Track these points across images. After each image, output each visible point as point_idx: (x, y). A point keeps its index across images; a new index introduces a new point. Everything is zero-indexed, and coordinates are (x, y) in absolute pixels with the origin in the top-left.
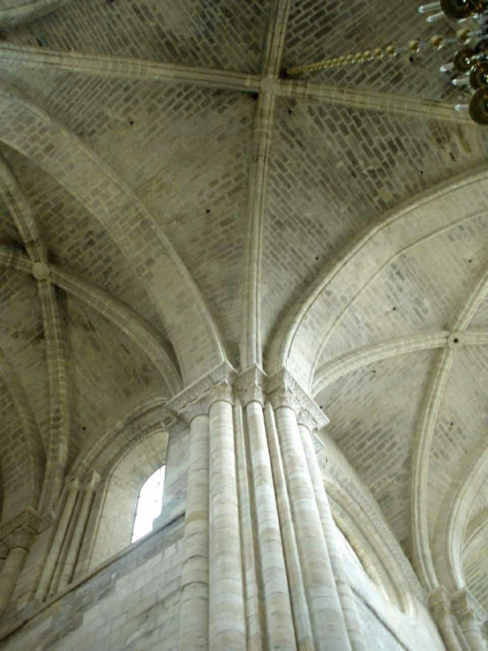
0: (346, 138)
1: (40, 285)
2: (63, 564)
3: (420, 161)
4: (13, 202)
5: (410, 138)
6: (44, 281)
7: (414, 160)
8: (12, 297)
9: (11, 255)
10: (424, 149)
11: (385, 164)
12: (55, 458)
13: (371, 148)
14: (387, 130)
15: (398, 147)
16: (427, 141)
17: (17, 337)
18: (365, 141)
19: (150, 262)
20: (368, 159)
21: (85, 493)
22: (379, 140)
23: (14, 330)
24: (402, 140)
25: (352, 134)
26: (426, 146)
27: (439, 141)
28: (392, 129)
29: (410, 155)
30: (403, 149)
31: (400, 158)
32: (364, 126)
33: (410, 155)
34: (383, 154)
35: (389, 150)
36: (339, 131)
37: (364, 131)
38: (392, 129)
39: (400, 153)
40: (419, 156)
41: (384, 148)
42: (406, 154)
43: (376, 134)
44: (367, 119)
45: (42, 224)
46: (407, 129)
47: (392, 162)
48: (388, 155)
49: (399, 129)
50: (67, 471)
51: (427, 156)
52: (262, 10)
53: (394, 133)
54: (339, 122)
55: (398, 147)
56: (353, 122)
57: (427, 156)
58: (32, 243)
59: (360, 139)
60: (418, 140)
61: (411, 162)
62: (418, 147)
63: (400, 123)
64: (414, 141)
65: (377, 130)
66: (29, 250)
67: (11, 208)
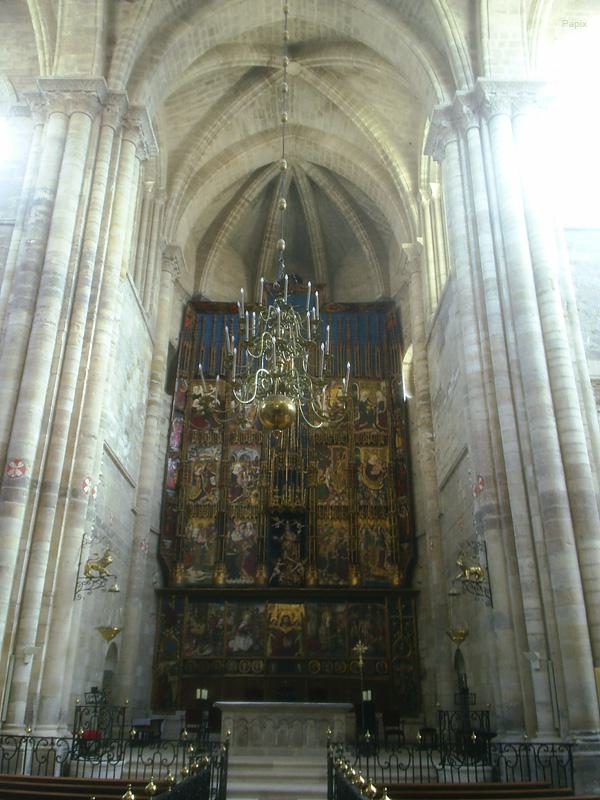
1: (302, 76)
2: (440, 276)
4: (231, 63)
6: (301, 72)
8: (295, 94)
9: (267, 80)
12: (402, 189)
17: (321, 114)
19: (348, 20)
21: (434, 204)
23: (316, 113)
45: (258, 47)
50: (416, 193)
58: (268, 63)
66: (273, 66)
67: (234, 65)
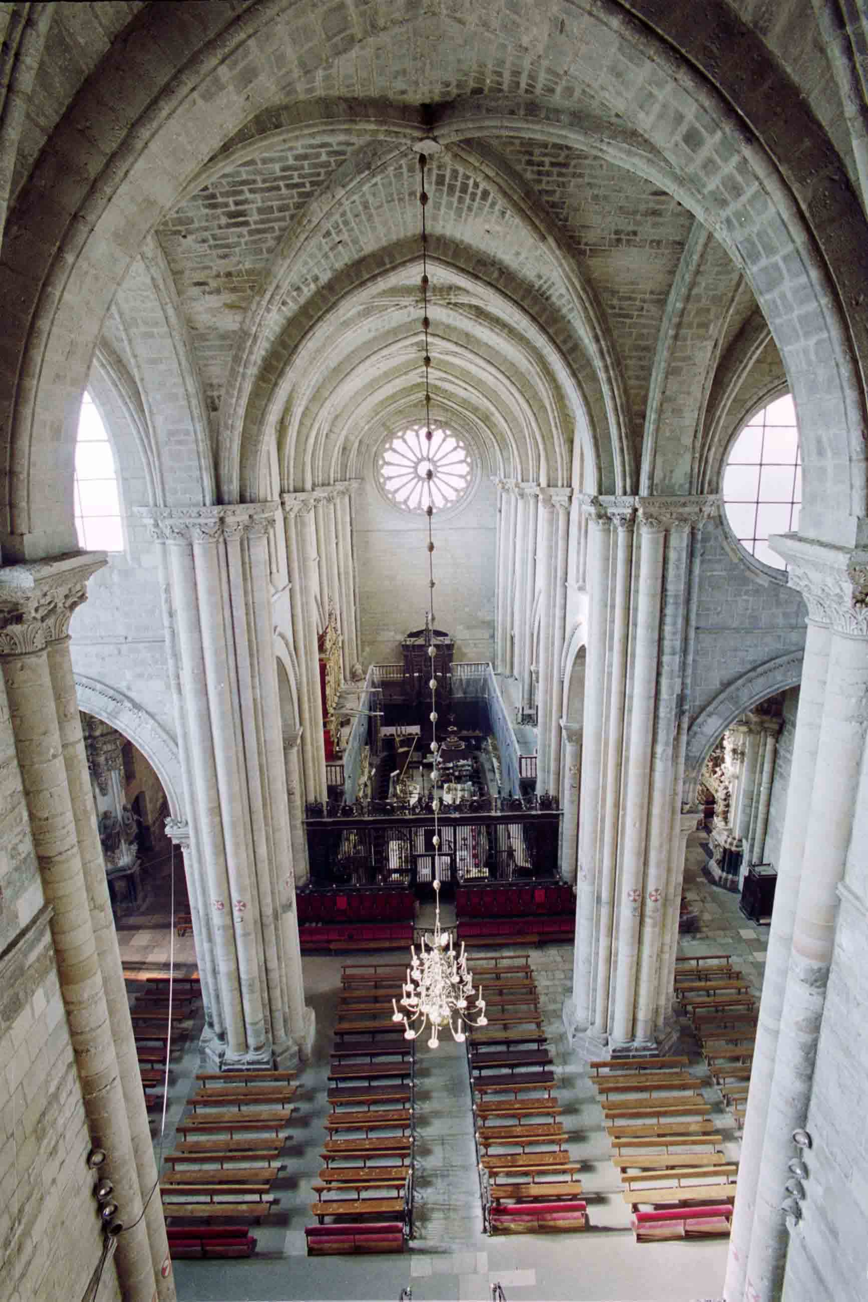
0: (277, 167)
3: (204, 241)
5: (243, 240)
7: (207, 234)
10: (221, 251)
11: (213, 196)
13: (245, 188)
14: (262, 217)
15: (233, 221)
16: (235, 259)
18: (260, 185)
20: (230, 179)
22: (253, 202)
24: (244, 230)
25: (279, 174)
26: (225, 256)
27: (229, 275)
28: (262, 222)
29: (217, 232)
30: (228, 226)
31: (218, 218)
32: (284, 191)
33: (217, 232)
34: (231, 200)
35: (233, 208)
36: (291, 162)
37: (278, 188)
38: (262, 222)
39: (224, 220)
40: (212, 242)
41: (237, 203)
42: (220, 227)
43: (263, 202)
44: (292, 197)
46: (254, 242)
47: (214, 206)
48: (226, 205)
49: (259, 231)
51: (208, 252)
52: (529, 168)
53: (256, 223)
54: (306, 167)
55: (233, 221)
56: (296, 180)
57: (208, 252)
59: (264, 181)
60: (237, 249)
61: (206, 229)
62: (227, 246)
63: (268, 235)
64: (238, 244)
65: (270, 203)
